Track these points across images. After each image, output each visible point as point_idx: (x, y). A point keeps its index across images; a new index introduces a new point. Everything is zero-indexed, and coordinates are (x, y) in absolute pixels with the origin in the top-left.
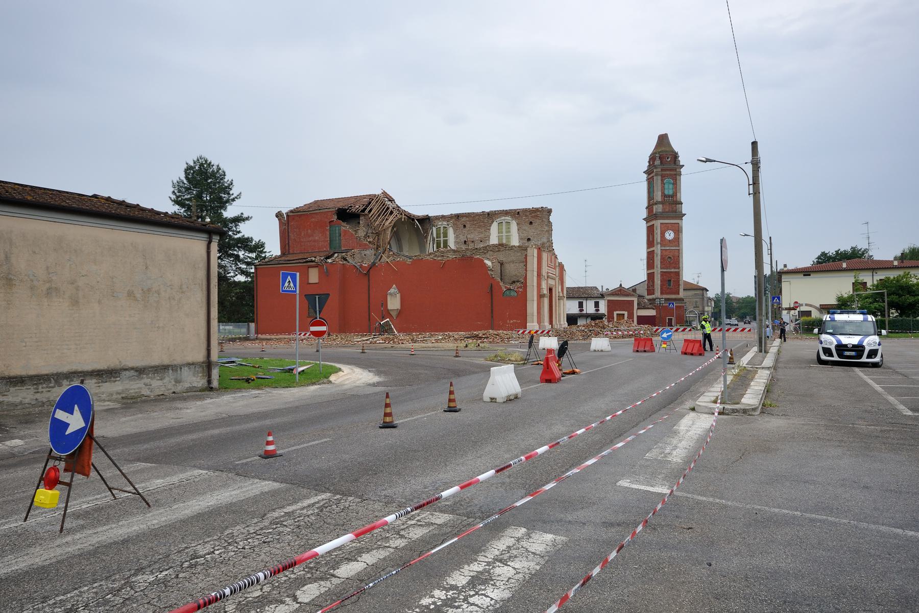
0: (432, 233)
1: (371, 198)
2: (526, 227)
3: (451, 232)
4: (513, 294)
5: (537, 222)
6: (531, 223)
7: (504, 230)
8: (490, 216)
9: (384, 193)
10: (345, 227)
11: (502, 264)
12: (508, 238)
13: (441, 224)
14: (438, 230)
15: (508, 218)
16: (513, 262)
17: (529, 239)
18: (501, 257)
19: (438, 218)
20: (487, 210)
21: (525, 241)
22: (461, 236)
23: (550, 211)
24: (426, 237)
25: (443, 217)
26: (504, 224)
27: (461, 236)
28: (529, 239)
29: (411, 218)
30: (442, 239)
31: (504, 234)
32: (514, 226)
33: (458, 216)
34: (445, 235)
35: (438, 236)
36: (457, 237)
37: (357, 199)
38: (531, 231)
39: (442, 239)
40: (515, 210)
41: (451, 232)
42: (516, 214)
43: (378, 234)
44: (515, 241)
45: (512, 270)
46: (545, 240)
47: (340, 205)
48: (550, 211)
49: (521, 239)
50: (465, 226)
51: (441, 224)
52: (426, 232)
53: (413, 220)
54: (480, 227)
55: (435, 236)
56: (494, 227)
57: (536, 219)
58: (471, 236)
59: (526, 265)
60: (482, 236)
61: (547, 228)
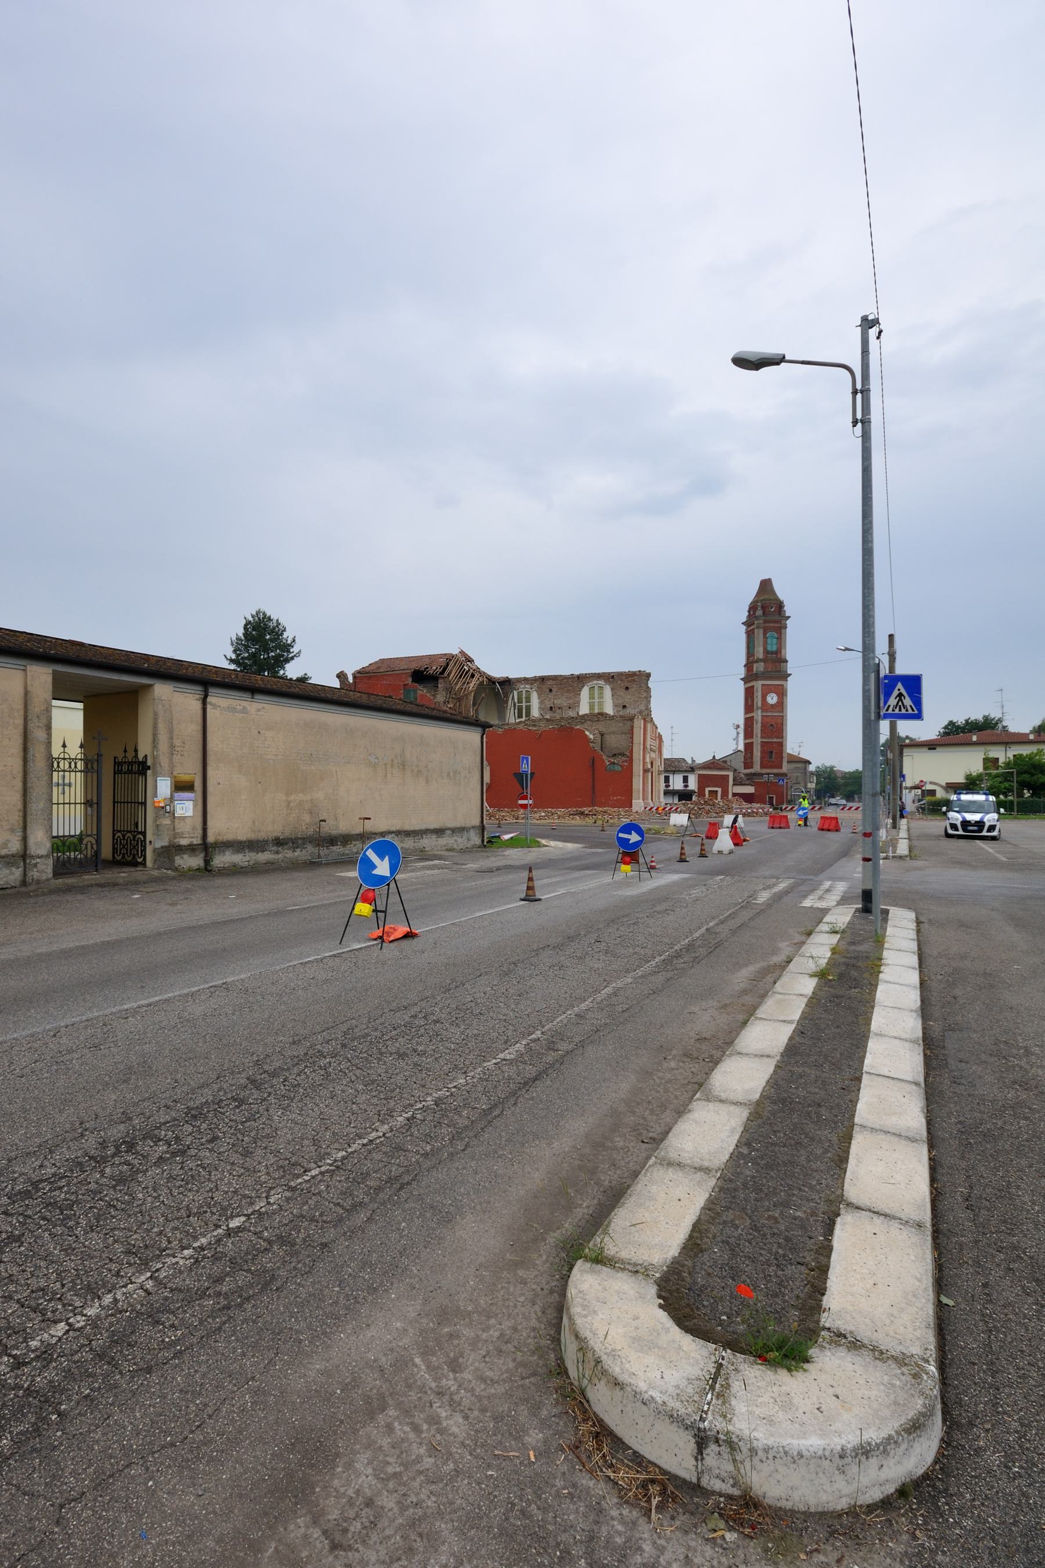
0: (513, 698)
1: (449, 658)
2: (622, 692)
3: (535, 698)
4: (618, 768)
5: (634, 687)
6: (627, 688)
7: (596, 696)
8: (581, 680)
9: (462, 652)
10: (422, 691)
11: (602, 735)
12: (601, 704)
13: (524, 688)
14: (520, 694)
15: (601, 682)
16: (614, 733)
17: (624, 707)
18: (602, 727)
19: (519, 680)
20: (577, 673)
21: (620, 708)
22: (546, 702)
23: (648, 675)
24: (507, 702)
25: (526, 680)
26: (596, 688)
27: (546, 702)
28: (624, 707)
29: (492, 681)
30: (524, 704)
31: (596, 700)
32: (608, 691)
33: (543, 679)
34: (528, 700)
35: (520, 701)
36: (541, 702)
37: (432, 658)
38: (627, 698)
39: (524, 704)
40: (609, 674)
41: (535, 698)
42: (610, 678)
43: (459, 700)
44: (609, 709)
45: (614, 741)
46: (643, 708)
47: (414, 666)
48: (648, 675)
49: (615, 706)
50: (551, 690)
51: (524, 688)
52: (506, 696)
53: (494, 683)
54: (568, 691)
55: (516, 700)
56: (585, 692)
57: (633, 684)
58: (558, 702)
59: (632, 738)
60: (571, 701)
61: (645, 694)
